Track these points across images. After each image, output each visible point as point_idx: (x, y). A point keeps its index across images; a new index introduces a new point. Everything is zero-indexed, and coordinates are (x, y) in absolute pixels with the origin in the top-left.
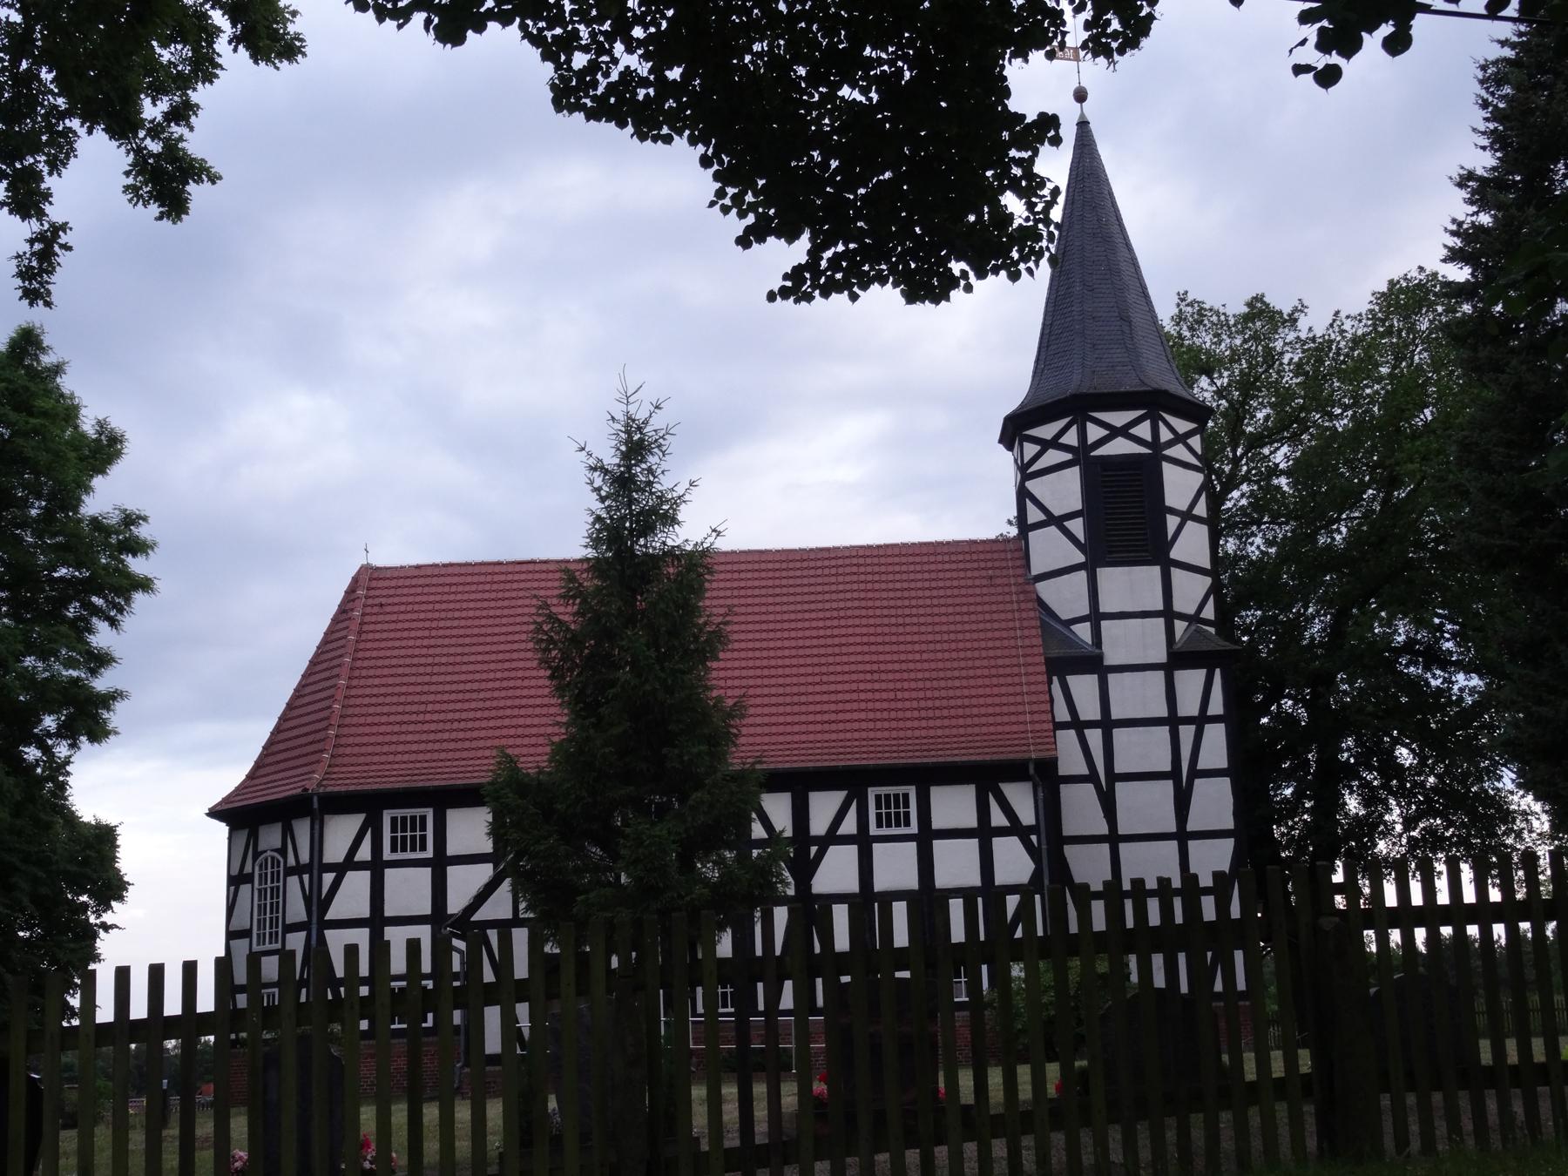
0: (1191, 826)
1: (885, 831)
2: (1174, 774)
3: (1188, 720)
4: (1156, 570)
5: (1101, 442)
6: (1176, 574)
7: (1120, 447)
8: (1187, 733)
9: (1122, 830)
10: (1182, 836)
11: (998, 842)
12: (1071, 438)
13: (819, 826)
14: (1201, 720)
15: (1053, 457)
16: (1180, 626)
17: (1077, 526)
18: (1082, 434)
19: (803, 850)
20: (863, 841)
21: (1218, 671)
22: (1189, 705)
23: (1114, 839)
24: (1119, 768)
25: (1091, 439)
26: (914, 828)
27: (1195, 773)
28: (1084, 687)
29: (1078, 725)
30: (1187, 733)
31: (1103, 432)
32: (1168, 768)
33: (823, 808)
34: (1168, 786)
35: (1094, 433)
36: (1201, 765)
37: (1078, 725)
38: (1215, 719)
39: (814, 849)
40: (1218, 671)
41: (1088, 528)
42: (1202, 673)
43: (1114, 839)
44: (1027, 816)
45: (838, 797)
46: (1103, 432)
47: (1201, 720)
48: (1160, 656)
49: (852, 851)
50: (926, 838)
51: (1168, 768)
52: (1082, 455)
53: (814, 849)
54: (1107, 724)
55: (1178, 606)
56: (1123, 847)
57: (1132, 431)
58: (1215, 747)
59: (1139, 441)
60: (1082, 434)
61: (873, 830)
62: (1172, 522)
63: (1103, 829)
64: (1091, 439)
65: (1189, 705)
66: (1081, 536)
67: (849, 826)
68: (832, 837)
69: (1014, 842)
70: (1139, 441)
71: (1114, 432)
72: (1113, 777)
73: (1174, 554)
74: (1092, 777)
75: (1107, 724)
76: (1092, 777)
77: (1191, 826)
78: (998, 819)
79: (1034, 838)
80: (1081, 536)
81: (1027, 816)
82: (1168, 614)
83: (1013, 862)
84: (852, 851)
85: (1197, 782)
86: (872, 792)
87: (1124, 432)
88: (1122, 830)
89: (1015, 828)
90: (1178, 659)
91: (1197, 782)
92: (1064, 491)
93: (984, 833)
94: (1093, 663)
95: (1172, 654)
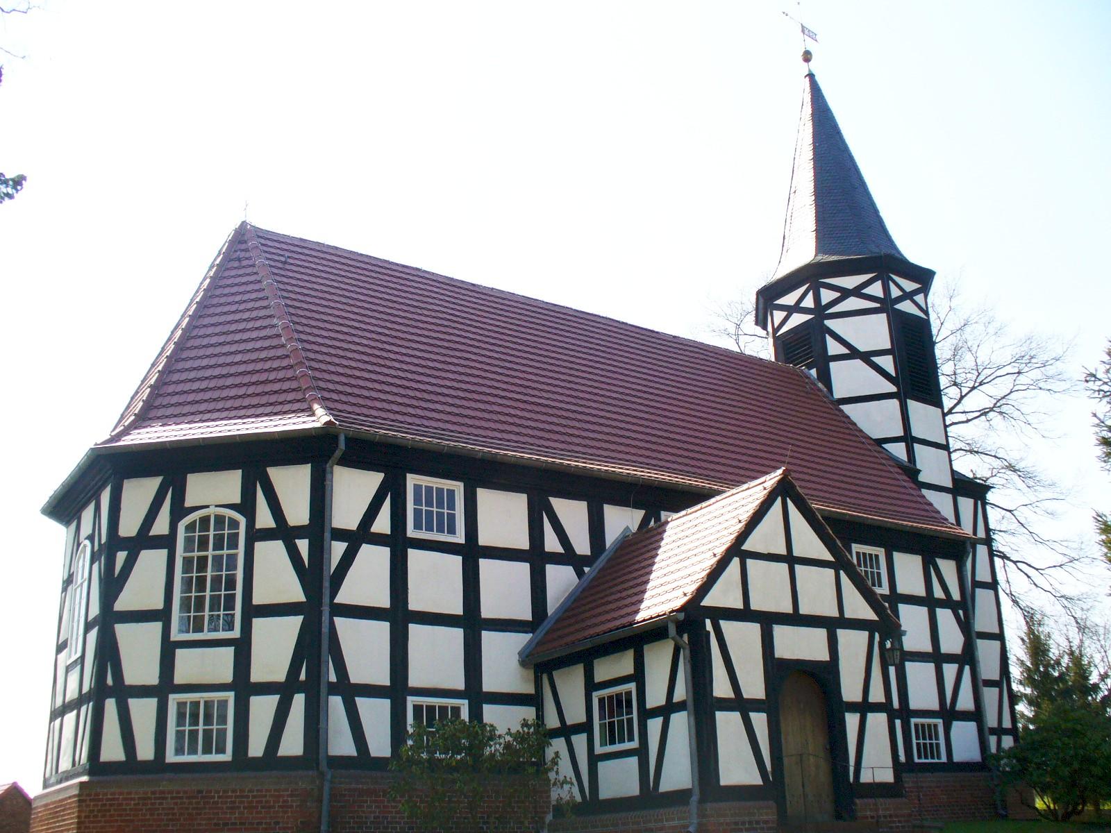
19: (318, 551)
45: (371, 481)
61: (411, 532)
68: (361, 536)
84: (385, 552)
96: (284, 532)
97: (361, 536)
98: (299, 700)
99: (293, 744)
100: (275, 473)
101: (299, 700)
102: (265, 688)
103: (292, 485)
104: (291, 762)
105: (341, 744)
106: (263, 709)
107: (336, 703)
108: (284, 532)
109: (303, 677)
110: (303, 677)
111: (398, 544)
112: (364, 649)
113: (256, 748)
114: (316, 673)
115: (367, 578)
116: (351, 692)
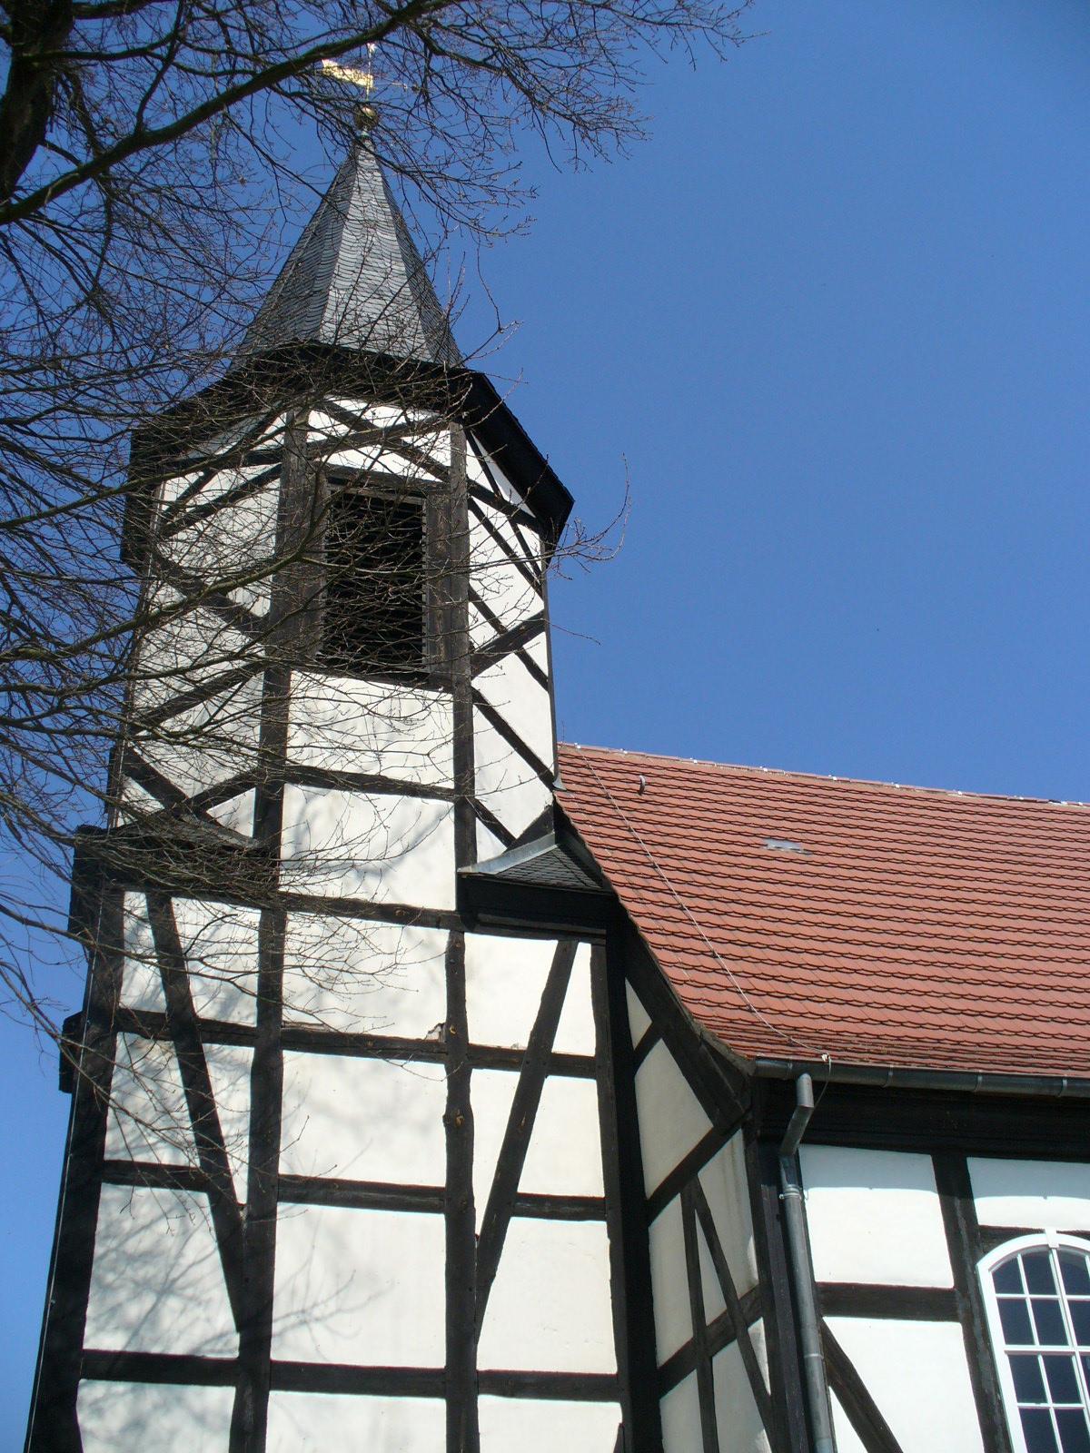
0: (491, 1355)
2: (450, 1199)
3: (498, 1058)
5: (336, 444)
8: (493, 1093)
9: (287, 1347)
14: (537, 1062)
21: (584, 951)
24: (296, 1159)
27: (508, 1200)
28: (219, 933)
29: (188, 1034)
30: (493, 1093)
34: (434, 1225)
36: (528, 1184)
37: (188, 1034)
38: (572, 1066)
40: (584, 951)
42: (545, 950)
47: (537, 1062)
54: (274, 1038)
58: (568, 1149)
65: (501, 1016)
72: (278, 1188)
74: (208, 1176)
75: (274, 1038)
76: (208, 1176)
77: (491, 1355)
85: (519, 1229)
87: (390, 439)
88: (291, 1344)
90: (487, 904)
91: (519, 1229)
94: (253, 874)
95: (467, 885)
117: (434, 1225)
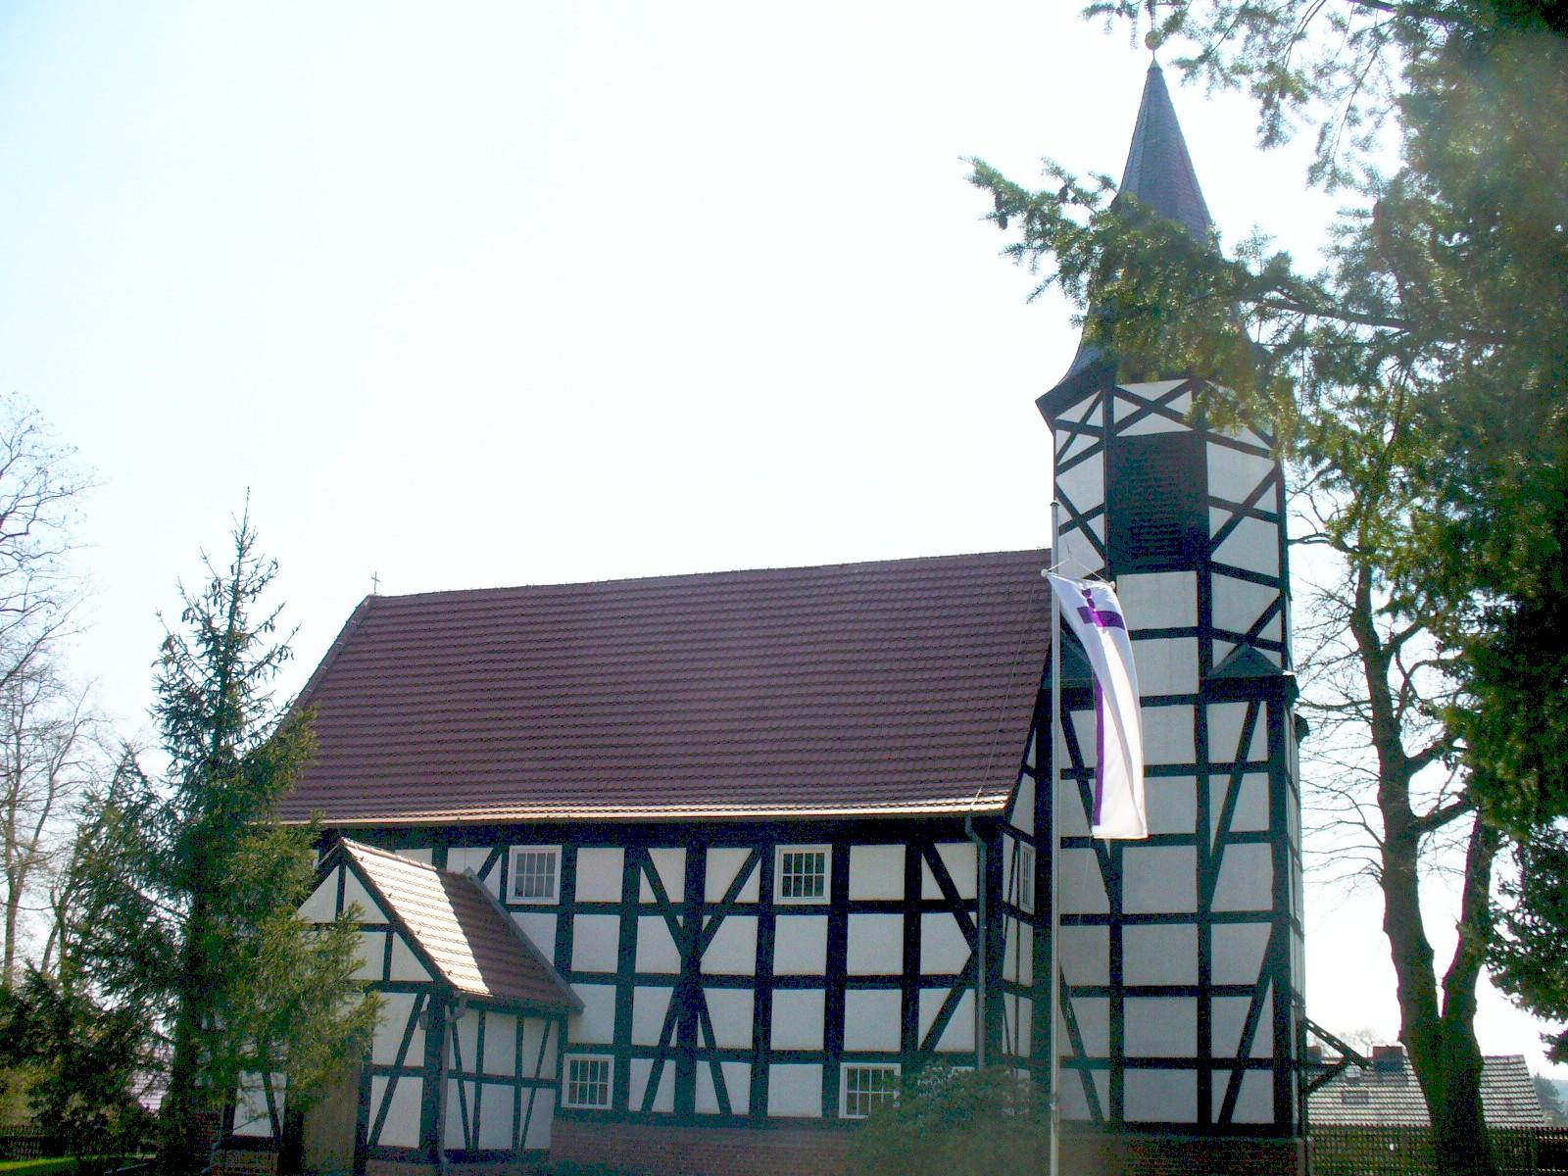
0: (1218, 905)
1: (792, 901)
2: (1199, 838)
4: (1191, 577)
6: (1219, 581)
7: (1154, 425)
10: (1204, 918)
11: (928, 920)
12: (1097, 419)
13: (715, 892)
15: (1084, 442)
16: (1221, 649)
17: (1098, 525)
18: (1109, 413)
20: (766, 914)
21: (1263, 707)
22: (1222, 749)
23: (1116, 921)
25: (1118, 416)
26: (825, 899)
27: (1227, 837)
31: (1133, 408)
32: (1192, 829)
33: (723, 864)
34: (1190, 853)
35: (1122, 409)
36: (1234, 827)
39: (706, 919)
40: (1263, 707)
41: (1110, 527)
42: (1241, 708)
43: (1116, 921)
44: (967, 887)
45: (738, 856)
46: (1133, 408)
48: (1192, 686)
49: (751, 923)
50: (840, 909)
51: (1192, 829)
52: (1110, 440)
53: (706, 919)
55: (1218, 622)
56: (1217, 930)
57: (1169, 405)
59: (1176, 416)
60: (1109, 413)
61: (779, 899)
62: (1217, 519)
63: (1103, 907)
64: (1118, 416)
65: (1222, 749)
66: (1101, 536)
67: (750, 893)
68: (730, 905)
69: (948, 920)
70: (1176, 416)
71: (1146, 407)
73: (1217, 557)
77: (1218, 905)
78: (930, 890)
79: (973, 915)
80: (1101, 536)
81: (967, 887)
82: (1205, 631)
83: (944, 945)
84: (751, 923)
85: (1230, 850)
86: (781, 851)
87: (1159, 406)
89: (951, 902)
91: (1230, 850)
92: (1089, 485)
93: (911, 907)
95: (1204, 683)
96: (662, 906)
97: (730, 905)
98: (670, 1066)
99: (664, 1102)
100: (656, 854)
101: (670, 1066)
102: (644, 1052)
103: (670, 863)
104: (661, 1118)
105: (706, 1101)
106: (640, 1068)
107: (703, 1069)
108: (662, 906)
109: (673, 1042)
110: (673, 1042)
111: (766, 914)
112: (730, 1016)
113: (635, 1103)
114: (687, 1033)
115: (732, 947)
116: (718, 1056)
117: (1190, 853)
